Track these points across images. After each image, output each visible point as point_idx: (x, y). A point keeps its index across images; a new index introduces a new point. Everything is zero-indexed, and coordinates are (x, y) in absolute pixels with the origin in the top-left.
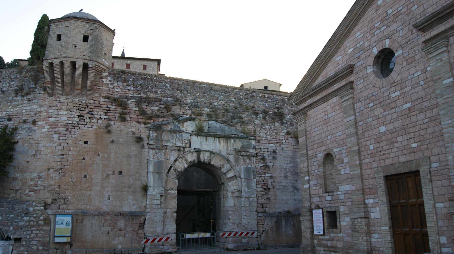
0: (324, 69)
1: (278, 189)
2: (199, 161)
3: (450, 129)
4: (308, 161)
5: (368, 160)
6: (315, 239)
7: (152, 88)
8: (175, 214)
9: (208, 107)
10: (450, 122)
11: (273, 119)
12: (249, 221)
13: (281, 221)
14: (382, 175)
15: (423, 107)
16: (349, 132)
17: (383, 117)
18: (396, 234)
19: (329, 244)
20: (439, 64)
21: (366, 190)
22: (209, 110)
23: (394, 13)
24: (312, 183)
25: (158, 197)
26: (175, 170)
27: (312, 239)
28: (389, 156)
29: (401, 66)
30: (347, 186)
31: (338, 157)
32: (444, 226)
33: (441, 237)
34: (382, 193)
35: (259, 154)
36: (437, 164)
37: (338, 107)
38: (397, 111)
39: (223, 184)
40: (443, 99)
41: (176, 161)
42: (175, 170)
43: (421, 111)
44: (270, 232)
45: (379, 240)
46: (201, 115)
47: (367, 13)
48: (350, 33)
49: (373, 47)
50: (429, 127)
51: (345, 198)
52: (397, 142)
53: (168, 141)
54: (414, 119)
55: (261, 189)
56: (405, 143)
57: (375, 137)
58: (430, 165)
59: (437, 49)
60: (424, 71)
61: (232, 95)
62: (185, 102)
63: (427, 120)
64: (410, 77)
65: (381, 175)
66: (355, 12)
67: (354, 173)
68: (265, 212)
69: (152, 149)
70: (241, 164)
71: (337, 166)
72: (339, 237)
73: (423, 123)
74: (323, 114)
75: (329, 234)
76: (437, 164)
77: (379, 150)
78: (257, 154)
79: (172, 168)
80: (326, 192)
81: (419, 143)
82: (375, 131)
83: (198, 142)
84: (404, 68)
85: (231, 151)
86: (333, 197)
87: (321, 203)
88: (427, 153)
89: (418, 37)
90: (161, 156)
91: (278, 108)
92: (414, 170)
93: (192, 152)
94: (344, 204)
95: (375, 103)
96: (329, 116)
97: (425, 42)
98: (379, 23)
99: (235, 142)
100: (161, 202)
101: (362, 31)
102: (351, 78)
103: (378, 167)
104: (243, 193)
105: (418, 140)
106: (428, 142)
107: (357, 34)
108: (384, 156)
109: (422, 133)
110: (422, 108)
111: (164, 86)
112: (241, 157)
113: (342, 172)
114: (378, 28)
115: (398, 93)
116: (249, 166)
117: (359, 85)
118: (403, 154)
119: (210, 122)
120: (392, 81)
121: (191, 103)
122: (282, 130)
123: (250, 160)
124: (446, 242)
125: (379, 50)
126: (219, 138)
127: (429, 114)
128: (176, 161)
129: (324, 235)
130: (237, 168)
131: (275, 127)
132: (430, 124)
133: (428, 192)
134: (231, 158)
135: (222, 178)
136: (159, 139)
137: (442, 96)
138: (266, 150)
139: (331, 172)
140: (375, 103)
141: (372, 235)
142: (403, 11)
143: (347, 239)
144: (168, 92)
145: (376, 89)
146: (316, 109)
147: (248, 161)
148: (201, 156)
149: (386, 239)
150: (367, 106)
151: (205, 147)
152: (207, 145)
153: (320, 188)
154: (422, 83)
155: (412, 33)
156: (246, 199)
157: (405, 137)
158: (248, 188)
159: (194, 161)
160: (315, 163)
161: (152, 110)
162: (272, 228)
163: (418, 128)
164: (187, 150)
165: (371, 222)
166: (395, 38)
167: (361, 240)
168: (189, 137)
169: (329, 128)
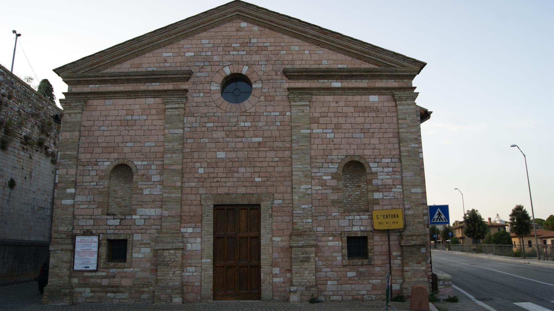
0: (137, 56)
3: (299, 173)
4: (77, 168)
5: (193, 184)
6: (75, 277)
10: (301, 166)
14: (213, 203)
15: (275, 146)
16: (171, 146)
17: (223, 142)
18: (217, 267)
19: (105, 282)
20: (300, 114)
21: (184, 217)
23: (259, 45)
27: (70, 277)
28: (224, 184)
29: (257, 100)
30: (153, 210)
31: (140, 173)
32: (279, 258)
33: (274, 268)
34: (208, 222)
36: (280, 202)
37: (154, 112)
38: (244, 141)
40: (299, 146)
43: (272, 149)
45: (195, 274)
47: (224, 26)
48: (194, 34)
49: (226, 66)
50: (277, 166)
51: (146, 224)
52: (238, 172)
54: (262, 154)
56: (249, 175)
57: (209, 161)
58: (273, 201)
59: (302, 100)
60: (283, 114)
63: (277, 159)
64: (265, 114)
65: (211, 204)
66: (212, 17)
67: (170, 195)
71: (137, 183)
72: (126, 272)
73: (272, 161)
74: (125, 112)
75: (106, 270)
76: (280, 202)
77: (211, 175)
80: (108, 215)
81: (263, 179)
82: (210, 155)
84: (261, 103)
86: (123, 221)
87: (96, 227)
88: (271, 190)
89: (282, 81)
92: (255, 203)
94: (143, 231)
95: (216, 124)
96: (135, 117)
97: (289, 89)
98: (239, 45)
101: (212, 41)
103: (206, 194)
105: (264, 175)
106: (274, 179)
107: (204, 41)
108: (218, 184)
109: (269, 169)
110: (273, 147)
113: (146, 192)
114: (235, 49)
115: (248, 124)
118: (243, 186)
120: (244, 110)
124: (278, 273)
125: (233, 72)
127: (280, 154)
132: (279, 164)
133: (267, 226)
137: (298, 142)
139: (115, 189)
140: (216, 124)
141: (185, 268)
142: (270, 48)
145: (221, 111)
146: (108, 102)
149: (206, 273)
150: (204, 125)
153: (97, 208)
154: (278, 124)
155: (276, 75)
157: (249, 169)
163: (265, 164)
165: (186, 254)
166: (255, 69)
167: (171, 275)
169: (132, 133)
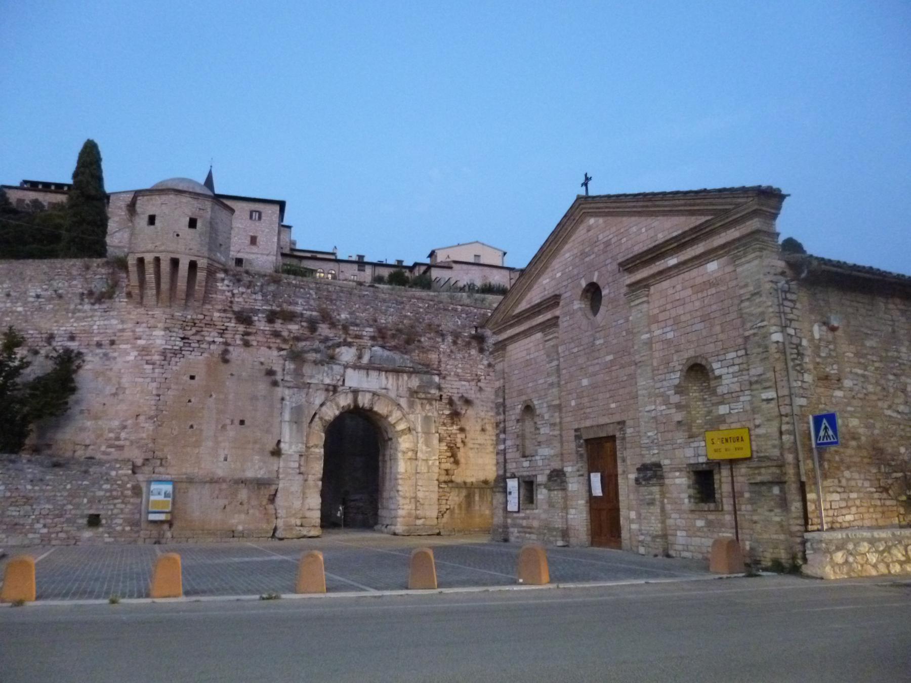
1: (471, 449)
2: (356, 406)
4: (504, 413)
5: (569, 419)
7: (290, 297)
8: (320, 483)
9: (371, 326)
11: (468, 344)
12: (427, 493)
13: (474, 496)
19: (524, 523)
22: (371, 330)
24: (509, 443)
25: (297, 457)
26: (321, 419)
27: (506, 518)
35: (444, 396)
37: (541, 346)
39: (391, 439)
41: (322, 405)
42: (321, 419)
44: (457, 511)
46: (359, 337)
53: (311, 377)
55: (446, 448)
59: (638, 297)
61: (407, 307)
62: (338, 317)
68: (452, 481)
69: (289, 387)
70: (418, 411)
78: (441, 396)
79: (317, 416)
83: (354, 379)
85: (403, 391)
90: (301, 397)
91: (476, 328)
93: (347, 393)
96: (532, 356)
99: (409, 377)
100: (300, 465)
102: (557, 312)
104: (419, 454)
107: (567, 255)
111: (307, 293)
112: (417, 400)
116: (430, 414)
117: (564, 323)
119: (373, 349)
121: (347, 319)
122: (481, 360)
123: (431, 404)
126: (386, 371)
128: (322, 405)
129: (518, 512)
130: (412, 417)
131: (470, 355)
134: (403, 402)
135: (389, 430)
136: (298, 373)
138: (455, 391)
143: (543, 516)
144: (312, 302)
147: (428, 407)
148: (360, 398)
151: (365, 385)
152: (368, 382)
156: (424, 463)
158: (427, 446)
159: (349, 405)
160: (513, 417)
161: (290, 332)
162: (460, 506)
164: (340, 389)
168: (342, 371)
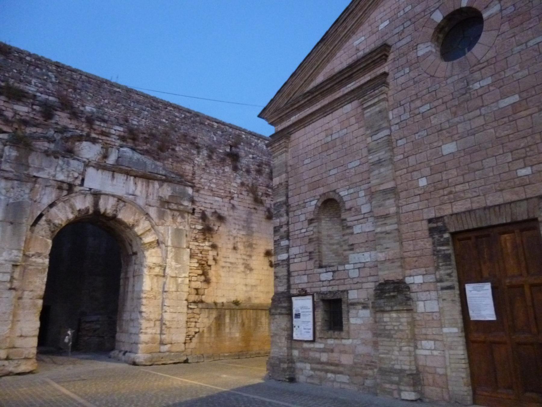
0: (328, 61)
1: (223, 267)
2: (97, 212)
4: (288, 215)
6: (296, 349)
7: (20, 72)
8: (40, 302)
9: (121, 125)
11: (223, 161)
12: (175, 315)
13: (224, 316)
18: (474, 342)
19: (324, 357)
22: (121, 129)
24: (294, 251)
25: (8, 267)
26: (49, 222)
27: (290, 348)
30: (367, 254)
35: (197, 210)
37: (353, 120)
39: (135, 254)
41: (51, 205)
42: (49, 222)
44: (206, 335)
45: (435, 353)
46: (107, 135)
51: (362, 275)
53: (40, 169)
55: (197, 265)
61: (163, 113)
62: (81, 108)
68: (202, 302)
69: (6, 179)
70: (168, 224)
72: (344, 345)
74: (323, 134)
75: (323, 341)
78: (194, 209)
79: (44, 218)
80: (321, 267)
83: (95, 180)
85: (153, 199)
86: (336, 274)
87: (310, 285)
90: (23, 192)
91: (231, 146)
92: (525, 217)
93: (85, 195)
94: (358, 286)
96: (334, 136)
99: (161, 186)
100: (12, 278)
102: (385, 68)
104: (168, 271)
108: (452, 196)
111: (43, 74)
112: (168, 211)
116: (181, 227)
119: (122, 149)
121: (93, 113)
122: (235, 178)
123: (183, 217)
126: (135, 177)
128: (51, 205)
129: (313, 341)
130: (161, 229)
131: (224, 172)
134: (153, 212)
135: (134, 243)
136: (21, 163)
138: (209, 206)
141: (419, 343)
143: (362, 349)
144: (50, 85)
146: (308, 129)
147: (179, 220)
148: (102, 202)
149: (452, 352)
150: (417, 112)
151: (108, 189)
152: (113, 185)
156: (172, 280)
158: (177, 261)
159: (87, 210)
160: (303, 218)
161: (16, 113)
162: (209, 328)
164: (77, 189)
165: (418, 318)
167: (396, 353)
168: (81, 168)
